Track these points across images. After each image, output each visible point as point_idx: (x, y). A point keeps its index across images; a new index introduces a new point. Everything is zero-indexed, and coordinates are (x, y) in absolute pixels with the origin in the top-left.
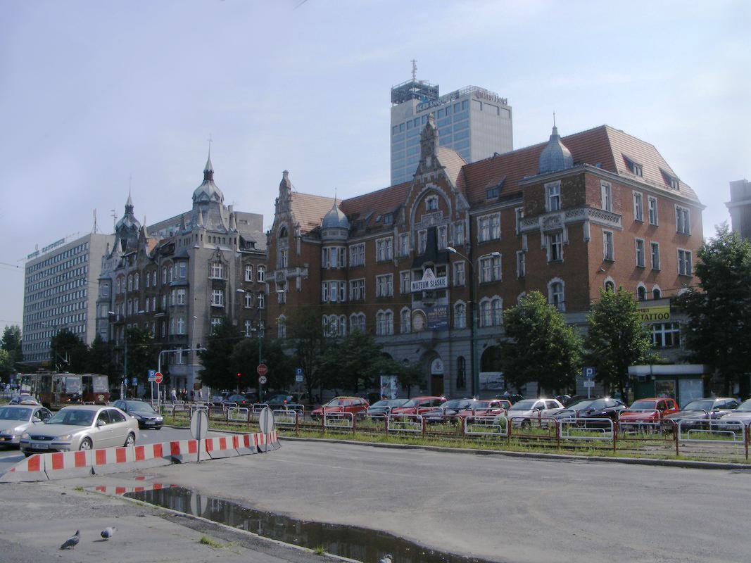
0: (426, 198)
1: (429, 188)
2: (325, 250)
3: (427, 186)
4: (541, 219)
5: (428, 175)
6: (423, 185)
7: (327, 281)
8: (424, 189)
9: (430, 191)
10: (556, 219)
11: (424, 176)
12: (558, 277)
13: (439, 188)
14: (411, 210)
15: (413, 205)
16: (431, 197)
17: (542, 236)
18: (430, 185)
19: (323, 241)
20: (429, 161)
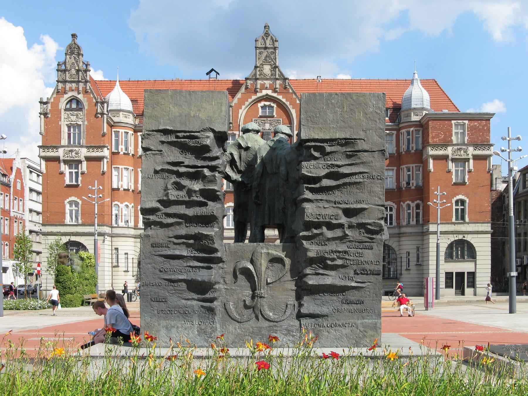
0: (274, 103)
1: (267, 95)
2: (117, 133)
3: (264, 92)
4: (450, 149)
5: (267, 83)
6: (258, 90)
7: (120, 167)
8: (259, 95)
9: (267, 98)
10: (465, 152)
11: (259, 82)
12: (463, 195)
13: (280, 97)
14: (240, 111)
15: (243, 107)
16: (267, 103)
17: (450, 163)
18: (270, 92)
19: (114, 122)
20: (267, 69)
